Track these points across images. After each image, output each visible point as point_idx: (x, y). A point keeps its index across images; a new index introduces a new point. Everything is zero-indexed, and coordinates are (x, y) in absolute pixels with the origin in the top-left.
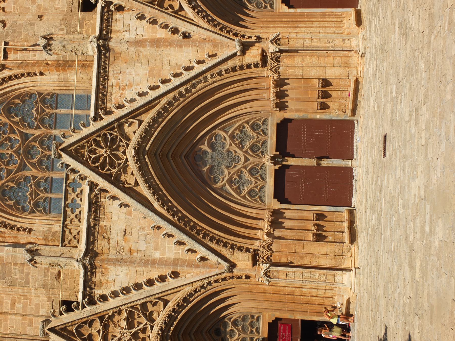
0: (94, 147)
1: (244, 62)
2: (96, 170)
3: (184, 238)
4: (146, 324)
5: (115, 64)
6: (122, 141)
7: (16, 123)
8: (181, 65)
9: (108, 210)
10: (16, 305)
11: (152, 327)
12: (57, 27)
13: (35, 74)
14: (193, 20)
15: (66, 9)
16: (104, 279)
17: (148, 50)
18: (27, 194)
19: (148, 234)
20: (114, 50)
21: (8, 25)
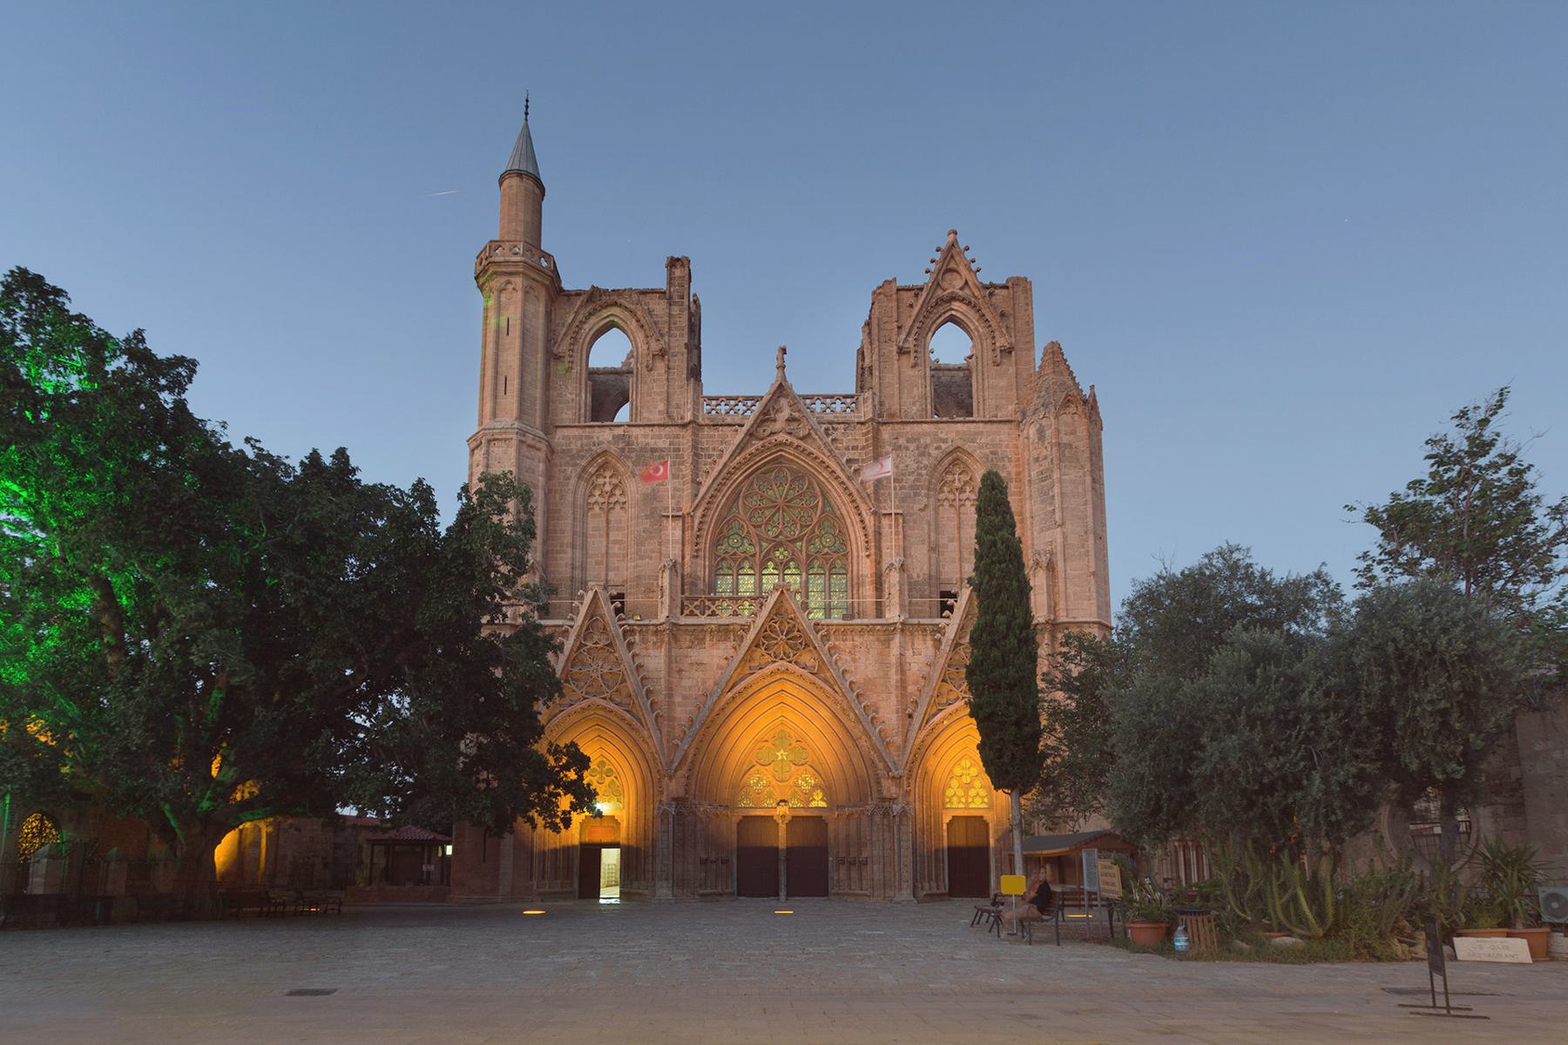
2: (763, 629)
9: (722, 645)
12: (921, 569)
17: (894, 677)
21: (922, 514)
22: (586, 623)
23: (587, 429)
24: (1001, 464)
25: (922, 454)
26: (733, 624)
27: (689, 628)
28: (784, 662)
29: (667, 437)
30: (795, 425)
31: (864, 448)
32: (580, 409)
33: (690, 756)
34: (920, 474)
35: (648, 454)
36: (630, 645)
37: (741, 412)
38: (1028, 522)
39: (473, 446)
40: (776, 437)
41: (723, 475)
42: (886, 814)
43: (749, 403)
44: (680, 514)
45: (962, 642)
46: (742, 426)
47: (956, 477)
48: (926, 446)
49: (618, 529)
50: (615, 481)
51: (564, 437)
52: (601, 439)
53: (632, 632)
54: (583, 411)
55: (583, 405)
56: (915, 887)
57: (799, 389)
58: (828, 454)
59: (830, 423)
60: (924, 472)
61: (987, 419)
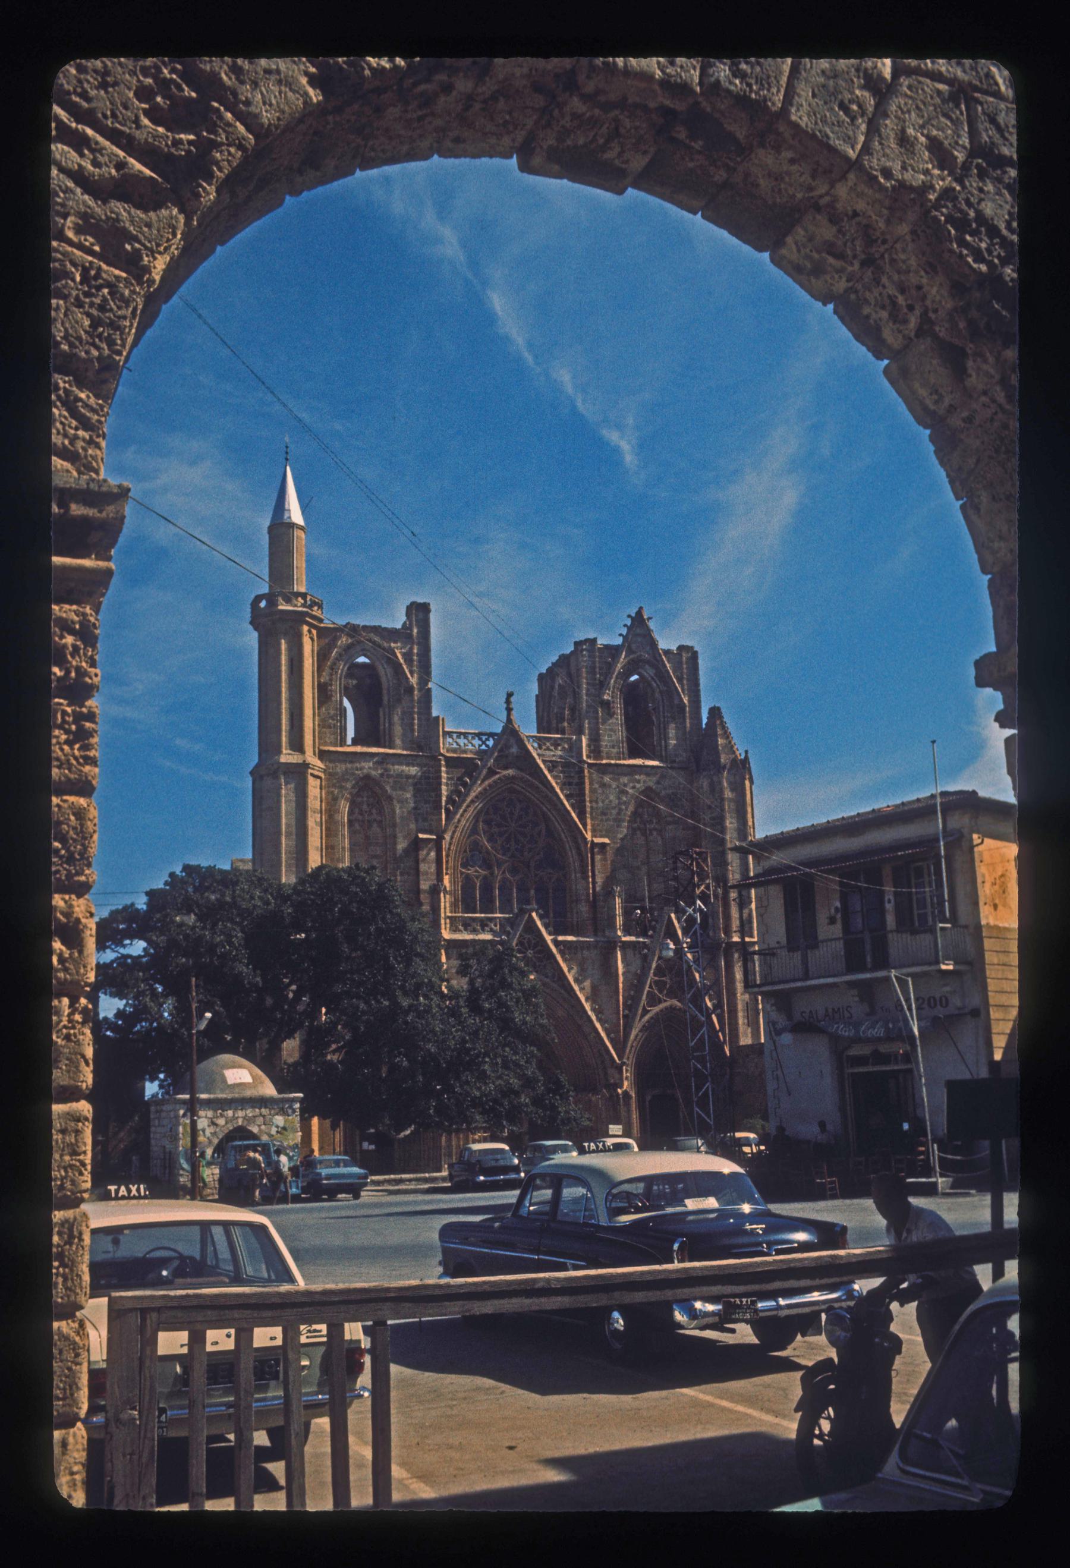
29: (418, 765)
31: (577, 784)
43: (484, 738)
48: (625, 785)
50: (371, 800)
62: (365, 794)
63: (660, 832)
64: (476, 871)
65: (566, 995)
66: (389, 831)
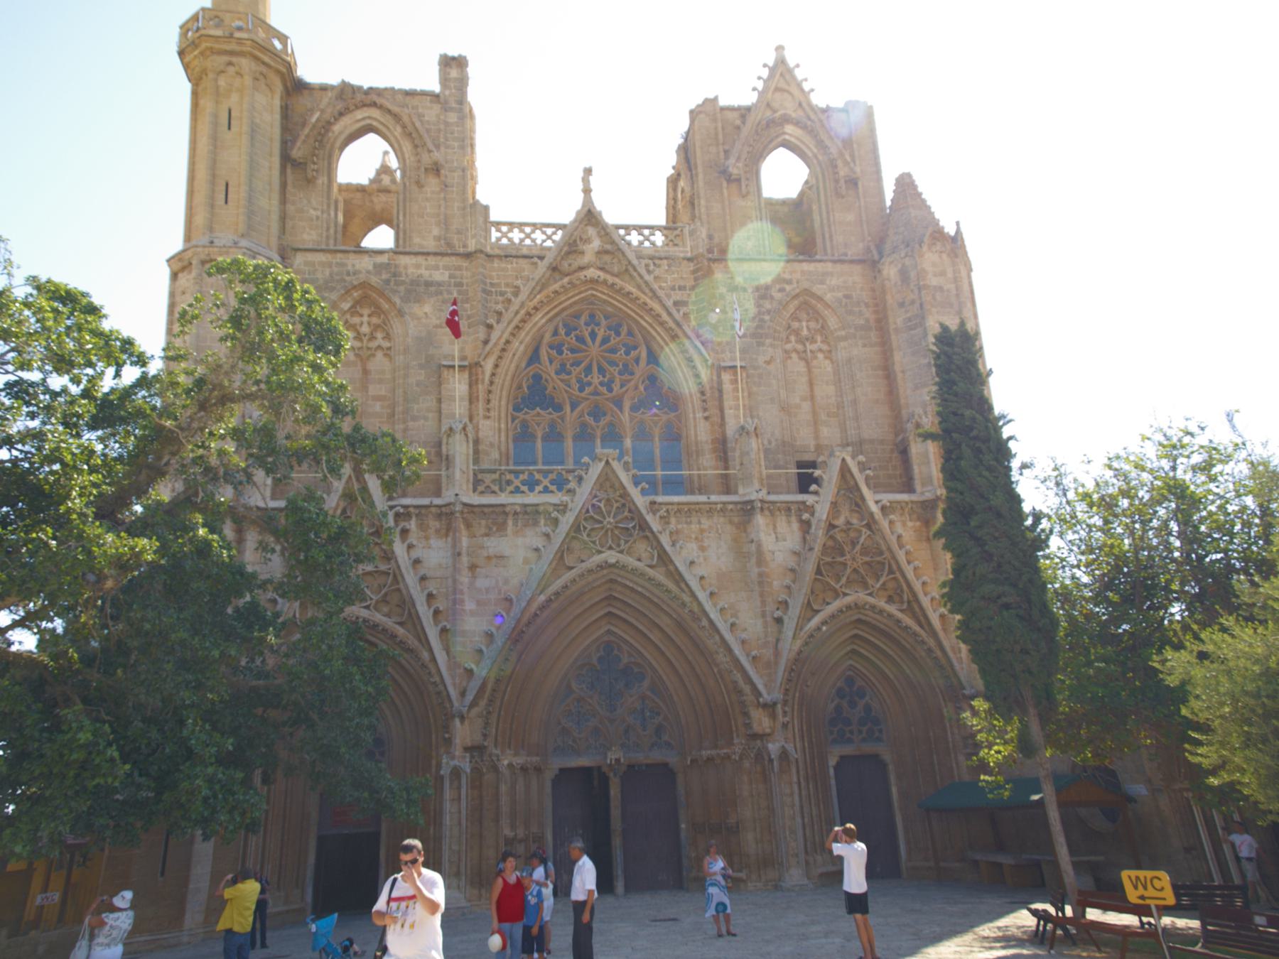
0: (616, 505)
1: (751, 708)
3: (499, 641)
4: (371, 599)
5: (729, 527)
6: (626, 542)
7: (636, 388)
8: (737, 618)
9: (529, 532)
10: (378, 403)
11: (367, 607)
13: (705, 410)
14: (801, 629)
15: (798, 443)
16: (431, 531)
18: (538, 409)
19: (500, 591)
20: (749, 522)
22: (342, 504)
23: (339, 255)
24: (856, 309)
25: (763, 297)
26: (543, 504)
27: (486, 510)
28: (613, 552)
29: (446, 268)
30: (607, 258)
32: (328, 229)
33: (489, 687)
34: (762, 320)
35: (422, 289)
36: (405, 532)
37: (539, 242)
38: (900, 376)
39: (177, 266)
40: (585, 273)
41: (519, 317)
42: (761, 756)
43: (549, 231)
44: (466, 363)
45: (836, 522)
46: (541, 258)
47: (804, 324)
49: (381, 381)
50: (375, 320)
51: (306, 263)
52: (358, 267)
53: (408, 516)
54: (332, 231)
55: (332, 225)
56: (807, 863)
57: (611, 216)
58: (650, 294)
59: (652, 258)
60: (767, 318)
61: (836, 258)
62: (366, 312)
63: (829, 355)
64: (538, 414)
65: (671, 585)
66: (400, 359)
